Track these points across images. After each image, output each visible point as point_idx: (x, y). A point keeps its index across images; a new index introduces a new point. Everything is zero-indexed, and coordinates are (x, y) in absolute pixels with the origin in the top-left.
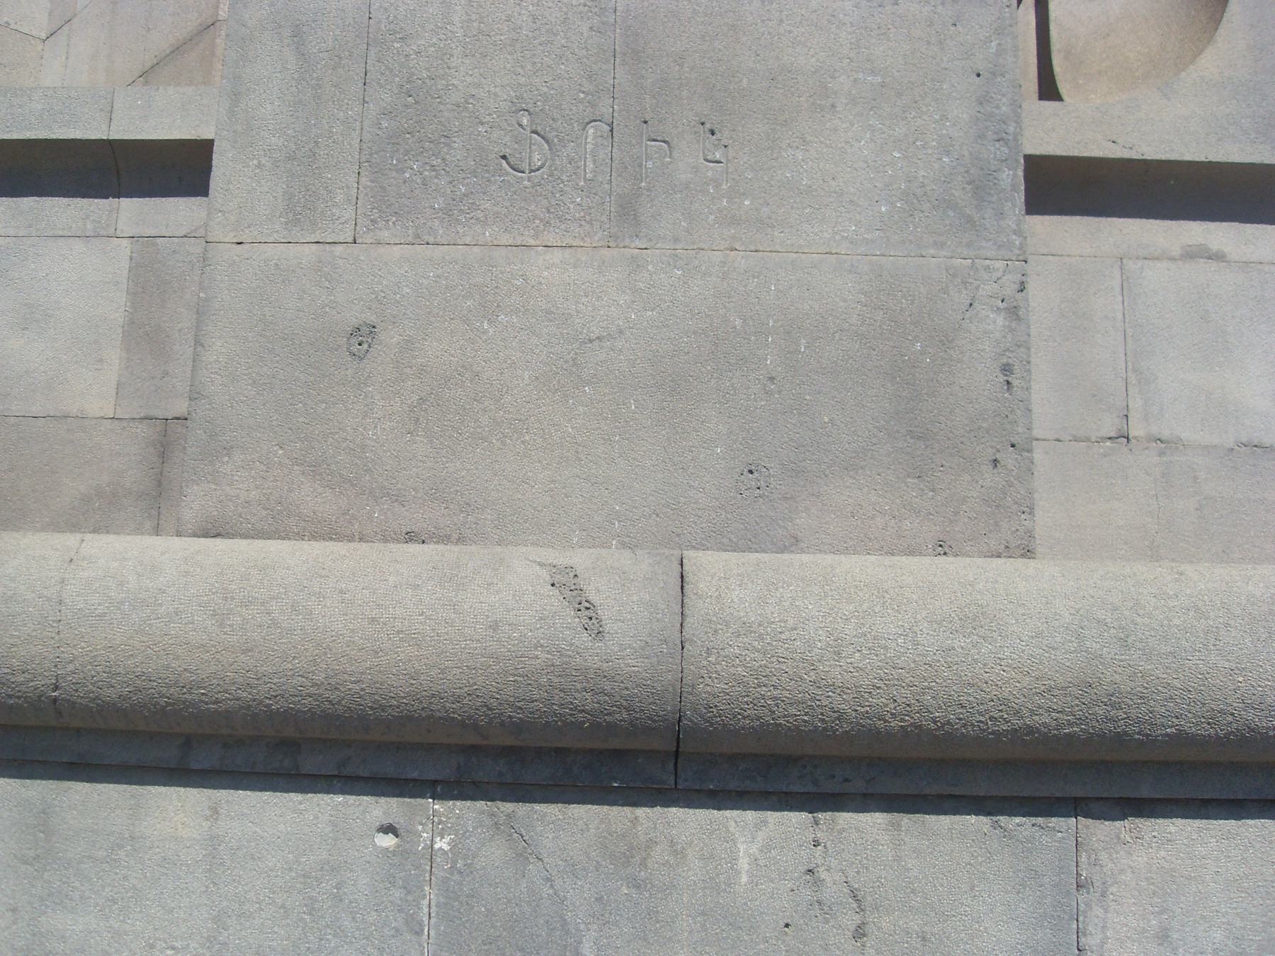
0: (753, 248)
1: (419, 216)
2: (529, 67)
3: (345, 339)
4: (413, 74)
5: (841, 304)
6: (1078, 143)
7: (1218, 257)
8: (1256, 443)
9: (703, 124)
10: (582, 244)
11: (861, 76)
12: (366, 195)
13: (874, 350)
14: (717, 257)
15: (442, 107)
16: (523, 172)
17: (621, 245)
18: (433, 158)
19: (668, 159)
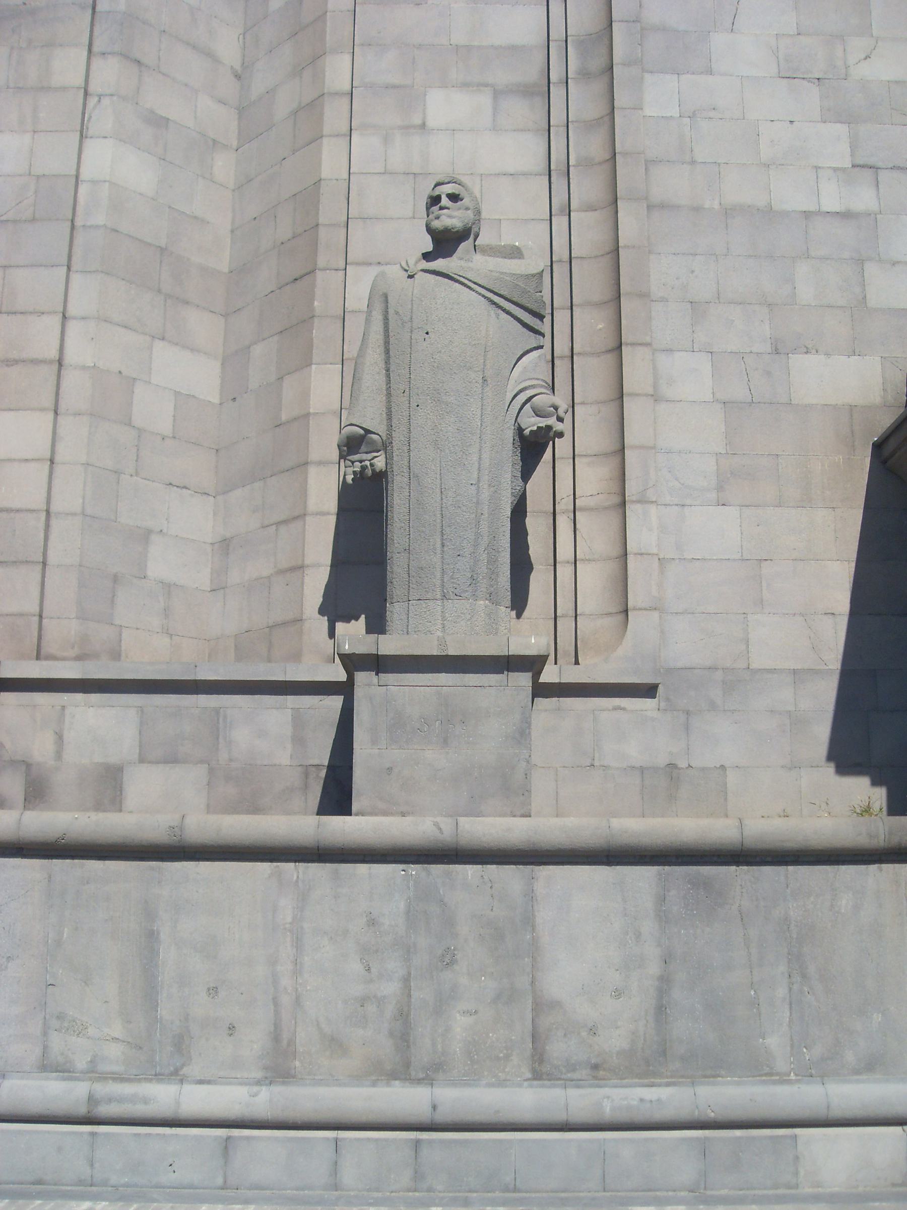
7: (624, 709)
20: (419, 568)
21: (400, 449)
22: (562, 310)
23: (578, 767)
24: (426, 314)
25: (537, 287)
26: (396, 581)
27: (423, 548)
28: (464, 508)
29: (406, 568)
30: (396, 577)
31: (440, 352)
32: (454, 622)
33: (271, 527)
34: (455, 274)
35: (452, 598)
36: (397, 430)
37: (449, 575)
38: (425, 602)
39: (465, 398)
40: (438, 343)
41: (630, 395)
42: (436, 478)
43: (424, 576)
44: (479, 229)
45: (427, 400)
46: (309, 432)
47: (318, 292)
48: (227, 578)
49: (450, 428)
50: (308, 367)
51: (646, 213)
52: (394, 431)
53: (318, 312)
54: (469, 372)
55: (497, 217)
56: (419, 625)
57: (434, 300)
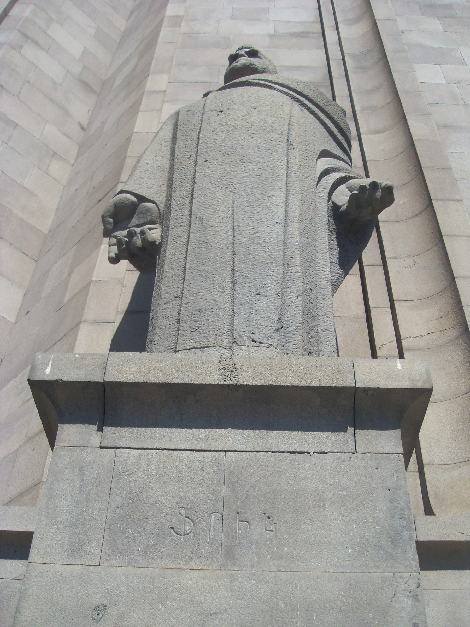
0: (289, 570)
1: (131, 554)
2: (185, 488)
3: (91, 612)
4: (132, 490)
5: (332, 596)
9: (264, 514)
10: (208, 568)
11: (336, 492)
12: (107, 543)
13: (349, 618)
14: (272, 574)
15: (145, 505)
16: (181, 535)
17: (227, 569)
18: (139, 527)
19: (248, 530)
20: (195, 310)
27: (204, 288)
30: (160, 330)
34: (254, 79)
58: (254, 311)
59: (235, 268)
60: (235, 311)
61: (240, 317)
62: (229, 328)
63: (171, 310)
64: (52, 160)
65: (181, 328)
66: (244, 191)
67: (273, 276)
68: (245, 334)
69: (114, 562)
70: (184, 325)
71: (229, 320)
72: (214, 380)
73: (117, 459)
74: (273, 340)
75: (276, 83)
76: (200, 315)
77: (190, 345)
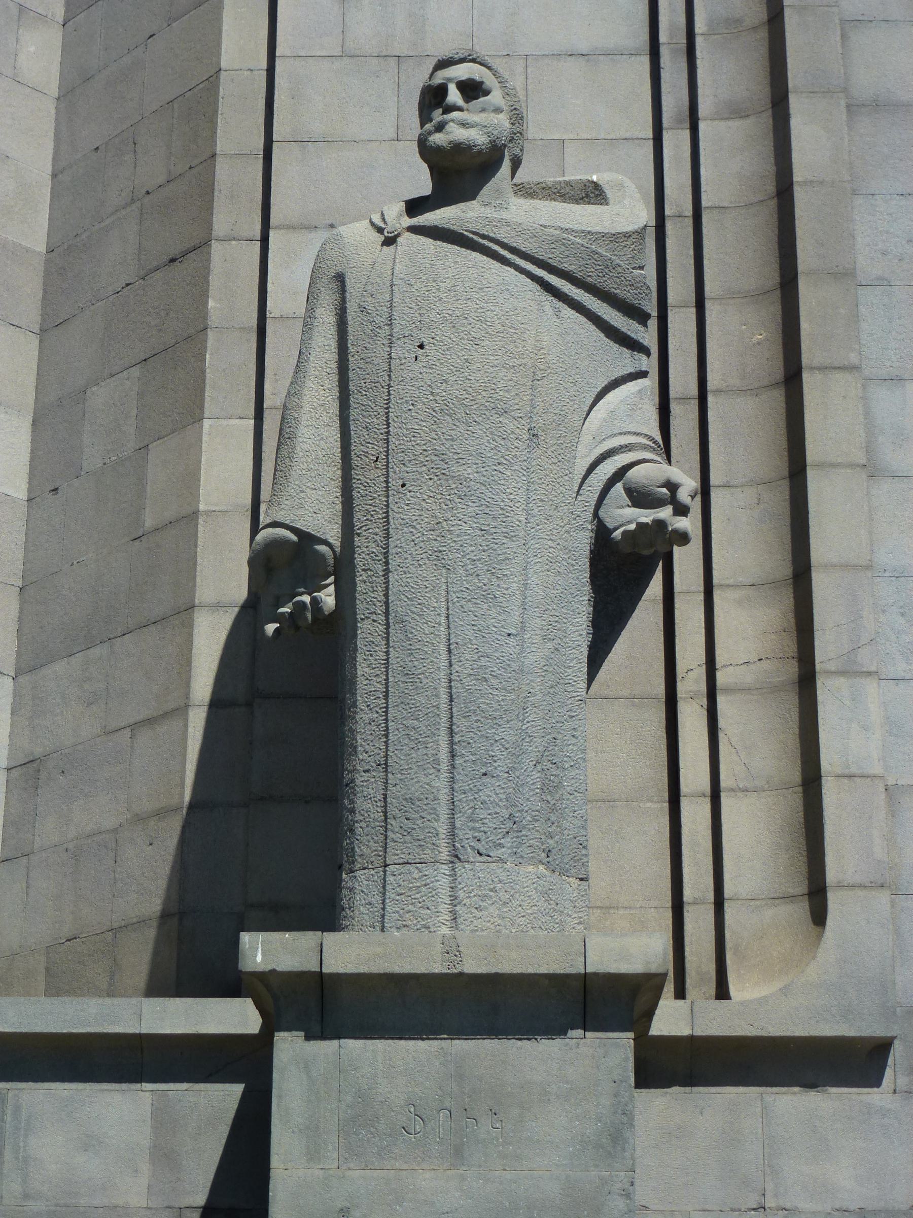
5: (552, 1194)
6: (730, 1027)
8: (844, 1209)
19: (476, 1128)
20: (406, 799)
21: (369, 569)
22: (682, 310)
23: (732, 1210)
24: (419, 309)
25: (633, 257)
26: (361, 827)
27: (414, 760)
28: (494, 682)
29: (380, 800)
30: (361, 818)
31: (446, 381)
32: (476, 908)
33: (120, 732)
35: (471, 859)
36: (364, 533)
37: (465, 813)
38: (417, 868)
39: (496, 470)
40: (442, 364)
41: (820, 465)
42: (440, 625)
43: (417, 816)
44: (522, 150)
45: (421, 473)
46: (196, 546)
47: (215, 281)
48: (34, 835)
49: (465, 527)
50: (196, 425)
51: (844, 117)
52: (359, 535)
53: (214, 319)
54: (501, 419)
55: (557, 136)
56: (407, 915)
57: (434, 284)
58: (479, 803)
59: (454, 727)
60: (455, 804)
61: (461, 814)
62: (449, 830)
63: (373, 787)
64: (21, 31)
65: (389, 827)
66: (462, 567)
67: (503, 741)
68: (468, 843)
69: (352, 1165)
70: (393, 822)
71: (449, 816)
72: (437, 968)
73: (342, 1051)
74: (503, 850)
75: (514, 251)
76: (412, 808)
77: (402, 858)
